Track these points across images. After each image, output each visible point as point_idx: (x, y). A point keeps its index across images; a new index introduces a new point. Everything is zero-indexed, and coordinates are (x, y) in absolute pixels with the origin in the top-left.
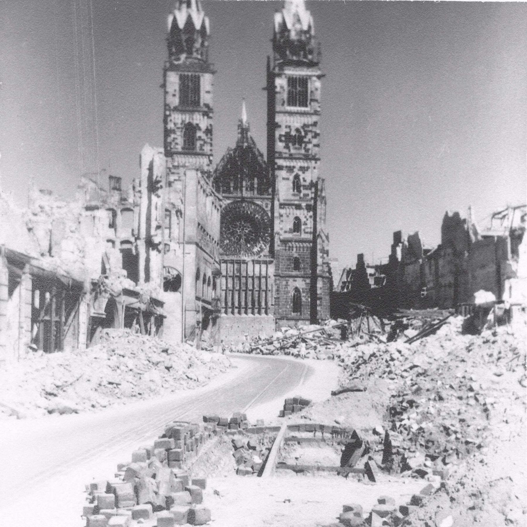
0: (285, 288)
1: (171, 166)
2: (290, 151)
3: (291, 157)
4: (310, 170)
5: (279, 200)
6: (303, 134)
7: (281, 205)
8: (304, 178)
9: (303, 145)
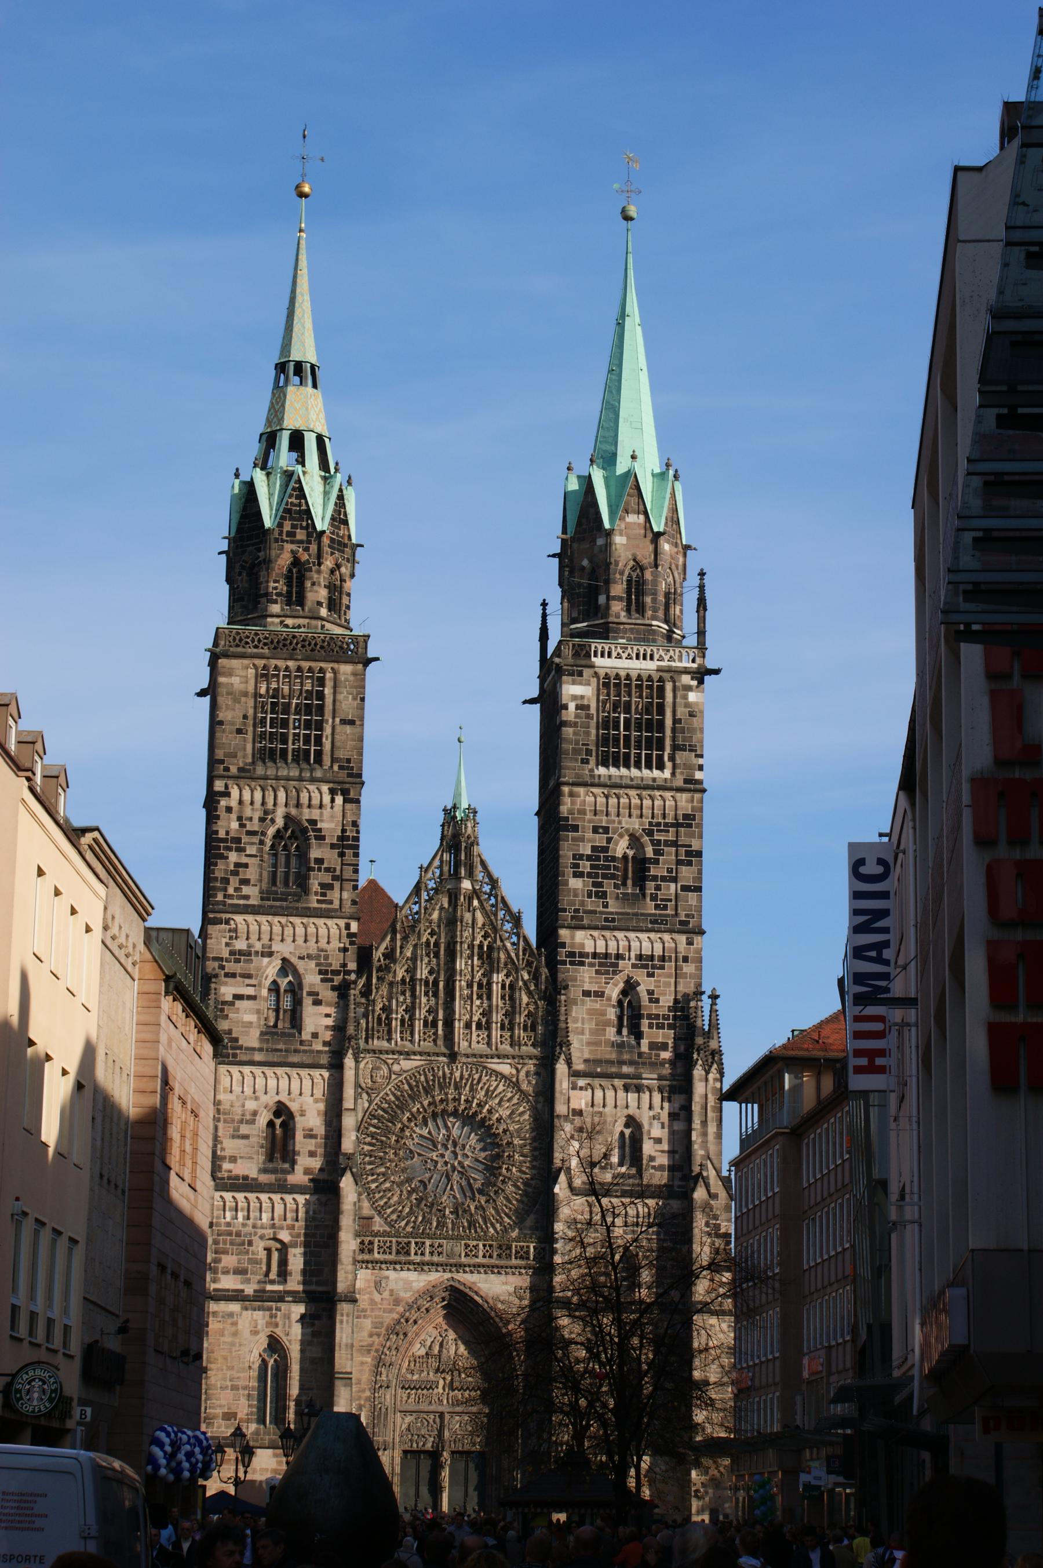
1: (225, 954)
2: (606, 906)
3: (610, 924)
4: (670, 966)
5: (569, 1063)
6: (649, 852)
7: (577, 1074)
8: (650, 993)
9: (650, 885)
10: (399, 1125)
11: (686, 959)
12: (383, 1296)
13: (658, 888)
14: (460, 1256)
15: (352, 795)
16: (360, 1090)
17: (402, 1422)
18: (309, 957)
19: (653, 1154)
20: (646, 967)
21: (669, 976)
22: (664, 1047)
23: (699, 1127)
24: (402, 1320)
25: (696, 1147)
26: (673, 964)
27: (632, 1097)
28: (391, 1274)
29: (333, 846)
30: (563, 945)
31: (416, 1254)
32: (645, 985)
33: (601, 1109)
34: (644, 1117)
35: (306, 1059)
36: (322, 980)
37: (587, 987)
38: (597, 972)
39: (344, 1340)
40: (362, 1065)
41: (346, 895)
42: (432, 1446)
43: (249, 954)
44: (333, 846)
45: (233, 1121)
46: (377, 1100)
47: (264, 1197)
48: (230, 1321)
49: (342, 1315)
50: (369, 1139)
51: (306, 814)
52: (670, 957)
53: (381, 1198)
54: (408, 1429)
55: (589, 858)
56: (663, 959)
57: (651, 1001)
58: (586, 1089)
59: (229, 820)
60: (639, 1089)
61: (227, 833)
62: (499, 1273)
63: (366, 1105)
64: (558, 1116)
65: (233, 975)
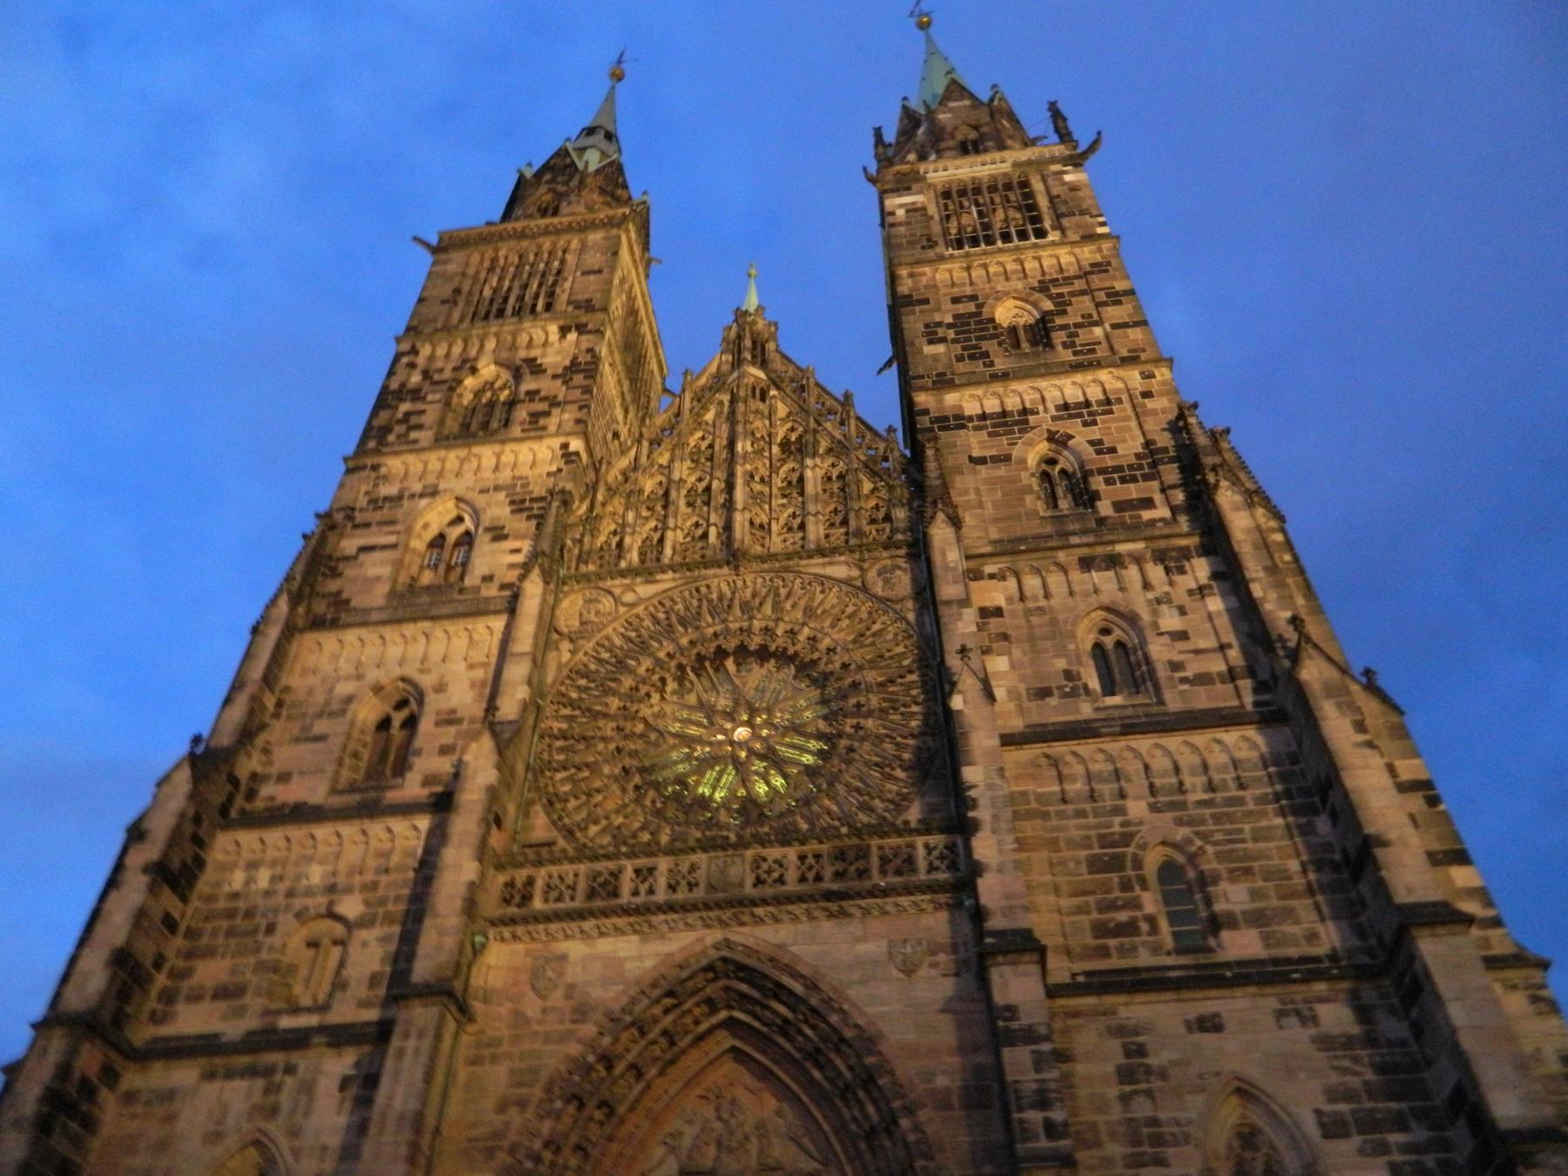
0: (1125, 1099)
1: (362, 501)
2: (992, 364)
5: (956, 522)
6: (1048, 305)
9: (1059, 337)
10: (628, 682)
11: (1147, 394)
12: (549, 1004)
13: (1071, 335)
14: (741, 885)
15: (590, 326)
16: (555, 636)
18: (497, 488)
19: (1177, 658)
20: (1080, 415)
21: (1127, 419)
22: (1148, 503)
23: (1261, 574)
25: (1268, 607)
26: (1127, 405)
27: (1103, 579)
28: (575, 949)
29: (555, 377)
30: (926, 412)
31: (636, 893)
32: (1081, 437)
33: (1043, 603)
34: (1139, 603)
35: (461, 609)
36: (513, 512)
37: (976, 453)
38: (990, 435)
39: (398, 1104)
40: (565, 604)
41: (566, 416)
43: (400, 497)
44: (555, 377)
45: (304, 715)
46: (589, 646)
47: (323, 831)
48: (159, 1111)
49: (406, 1036)
50: (566, 711)
51: (522, 354)
52: (1119, 401)
53: (578, 809)
55: (949, 326)
56: (1108, 402)
57: (1099, 452)
58: (1004, 578)
59: (409, 376)
60: (1114, 562)
61: (403, 385)
62: (844, 914)
63: (566, 656)
64: (949, 603)
65: (367, 525)
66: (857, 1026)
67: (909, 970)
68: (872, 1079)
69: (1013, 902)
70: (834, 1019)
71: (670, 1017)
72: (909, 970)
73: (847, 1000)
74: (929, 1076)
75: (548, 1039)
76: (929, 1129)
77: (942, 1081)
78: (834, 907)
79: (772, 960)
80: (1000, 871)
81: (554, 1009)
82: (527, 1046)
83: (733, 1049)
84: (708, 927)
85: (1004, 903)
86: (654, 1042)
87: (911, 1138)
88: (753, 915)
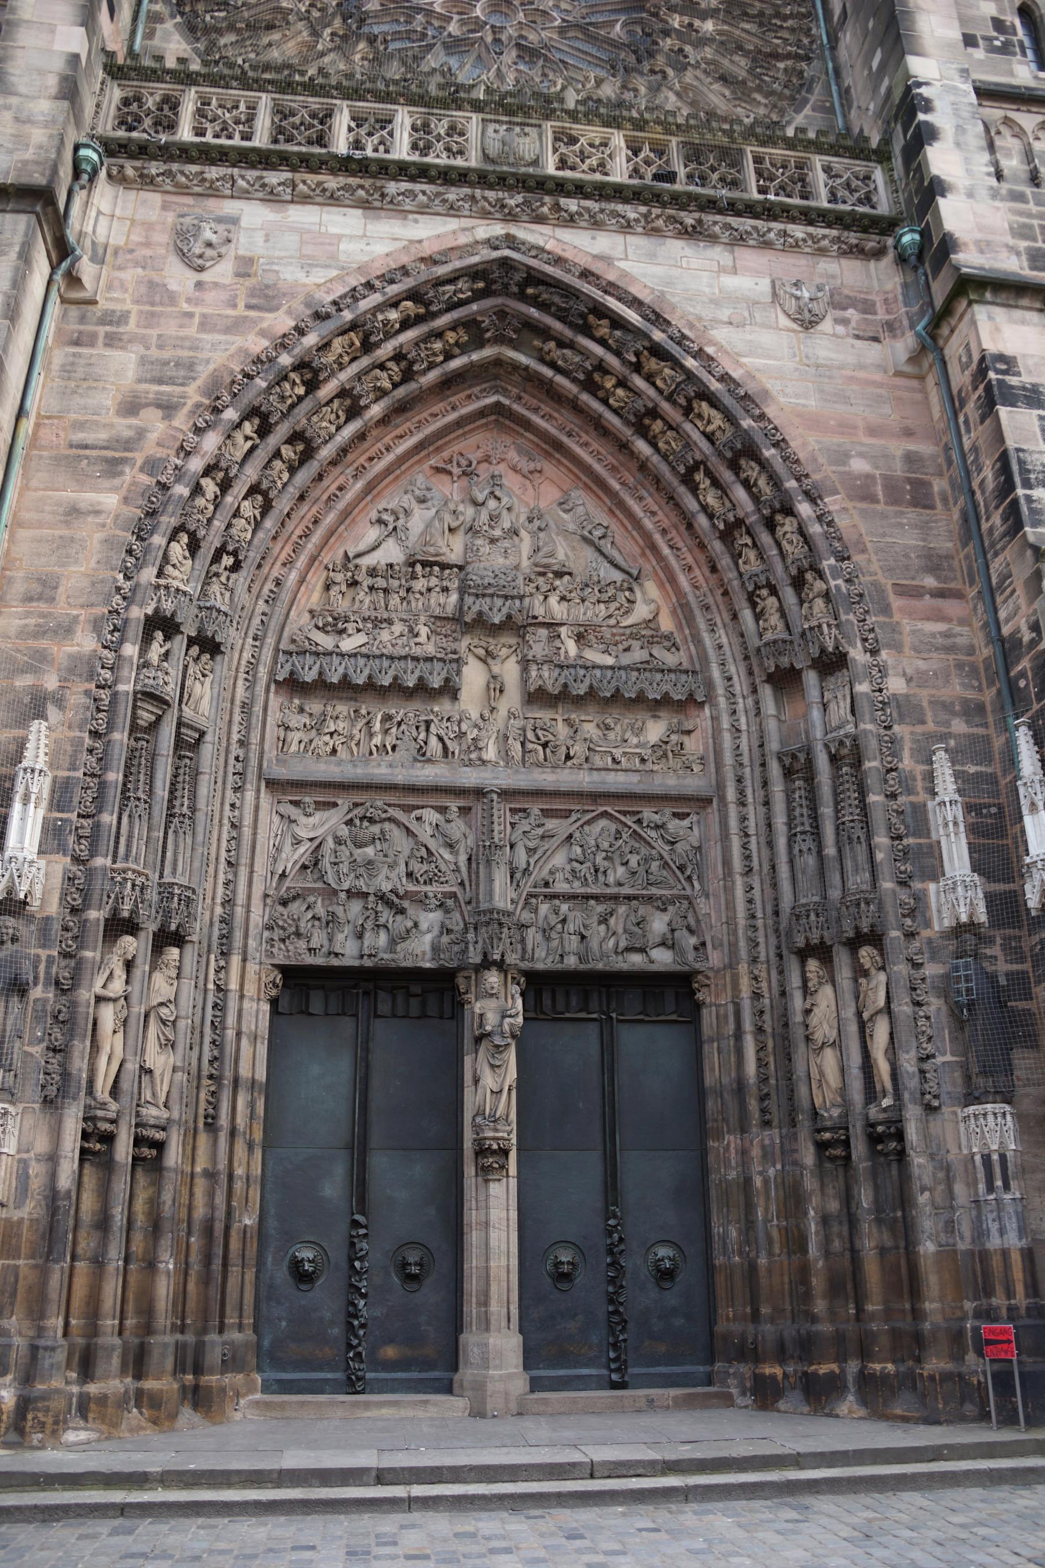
17: (278, 839)
24: (286, 360)
28: (253, 215)
42: (436, 949)
54: (312, 865)
66: (724, 378)
67: (808, 322)
68: (751, 452)
69: (990, 237)
70: (690, 363)
71: (410, 335)
72: (808, 322)
73: (712, 343)
74: (842, 457)
75: (205, 325)
76: (842, 522)
77: (859, 466)
78: (689, 219)
79: (586, 274)
80: (970, 195)
81: (216, 285)
82: (170, 328)
83: (498, 404)
84: (485, 215)
85: (979, 236)
86: (382, 367)
87: (815, 529)
88: (557, 208)
